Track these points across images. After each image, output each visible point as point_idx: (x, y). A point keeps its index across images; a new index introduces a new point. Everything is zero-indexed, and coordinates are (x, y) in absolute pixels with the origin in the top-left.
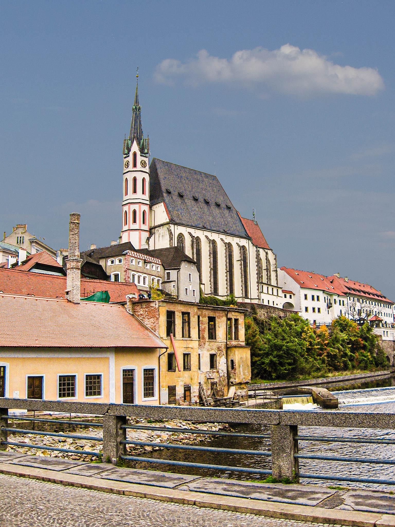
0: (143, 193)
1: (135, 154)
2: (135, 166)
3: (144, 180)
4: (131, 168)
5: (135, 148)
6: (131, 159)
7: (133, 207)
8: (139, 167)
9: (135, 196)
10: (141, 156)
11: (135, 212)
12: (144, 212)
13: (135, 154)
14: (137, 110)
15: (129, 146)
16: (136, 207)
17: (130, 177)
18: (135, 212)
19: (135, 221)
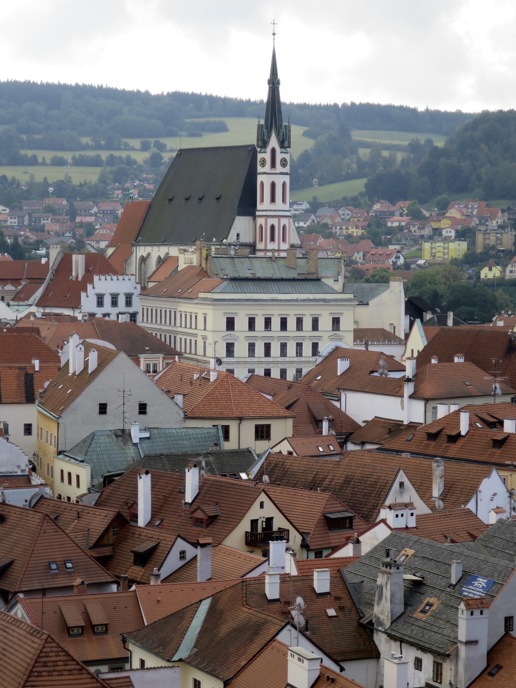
0: (283, 202)
1: (273, 151)
2: (273, 165)
3: (284, 184)
4: (267, 168)
5: (274, 142)
6: (267, 156)
7: (271, 221)
8: (279, 168)
9: (273, 207)
10: (282, 152)
11: (273, 227)
13: (273, 151)
14: (274, 83)
15: (265, 138)
16: (274, 221)
18: (273, 227)
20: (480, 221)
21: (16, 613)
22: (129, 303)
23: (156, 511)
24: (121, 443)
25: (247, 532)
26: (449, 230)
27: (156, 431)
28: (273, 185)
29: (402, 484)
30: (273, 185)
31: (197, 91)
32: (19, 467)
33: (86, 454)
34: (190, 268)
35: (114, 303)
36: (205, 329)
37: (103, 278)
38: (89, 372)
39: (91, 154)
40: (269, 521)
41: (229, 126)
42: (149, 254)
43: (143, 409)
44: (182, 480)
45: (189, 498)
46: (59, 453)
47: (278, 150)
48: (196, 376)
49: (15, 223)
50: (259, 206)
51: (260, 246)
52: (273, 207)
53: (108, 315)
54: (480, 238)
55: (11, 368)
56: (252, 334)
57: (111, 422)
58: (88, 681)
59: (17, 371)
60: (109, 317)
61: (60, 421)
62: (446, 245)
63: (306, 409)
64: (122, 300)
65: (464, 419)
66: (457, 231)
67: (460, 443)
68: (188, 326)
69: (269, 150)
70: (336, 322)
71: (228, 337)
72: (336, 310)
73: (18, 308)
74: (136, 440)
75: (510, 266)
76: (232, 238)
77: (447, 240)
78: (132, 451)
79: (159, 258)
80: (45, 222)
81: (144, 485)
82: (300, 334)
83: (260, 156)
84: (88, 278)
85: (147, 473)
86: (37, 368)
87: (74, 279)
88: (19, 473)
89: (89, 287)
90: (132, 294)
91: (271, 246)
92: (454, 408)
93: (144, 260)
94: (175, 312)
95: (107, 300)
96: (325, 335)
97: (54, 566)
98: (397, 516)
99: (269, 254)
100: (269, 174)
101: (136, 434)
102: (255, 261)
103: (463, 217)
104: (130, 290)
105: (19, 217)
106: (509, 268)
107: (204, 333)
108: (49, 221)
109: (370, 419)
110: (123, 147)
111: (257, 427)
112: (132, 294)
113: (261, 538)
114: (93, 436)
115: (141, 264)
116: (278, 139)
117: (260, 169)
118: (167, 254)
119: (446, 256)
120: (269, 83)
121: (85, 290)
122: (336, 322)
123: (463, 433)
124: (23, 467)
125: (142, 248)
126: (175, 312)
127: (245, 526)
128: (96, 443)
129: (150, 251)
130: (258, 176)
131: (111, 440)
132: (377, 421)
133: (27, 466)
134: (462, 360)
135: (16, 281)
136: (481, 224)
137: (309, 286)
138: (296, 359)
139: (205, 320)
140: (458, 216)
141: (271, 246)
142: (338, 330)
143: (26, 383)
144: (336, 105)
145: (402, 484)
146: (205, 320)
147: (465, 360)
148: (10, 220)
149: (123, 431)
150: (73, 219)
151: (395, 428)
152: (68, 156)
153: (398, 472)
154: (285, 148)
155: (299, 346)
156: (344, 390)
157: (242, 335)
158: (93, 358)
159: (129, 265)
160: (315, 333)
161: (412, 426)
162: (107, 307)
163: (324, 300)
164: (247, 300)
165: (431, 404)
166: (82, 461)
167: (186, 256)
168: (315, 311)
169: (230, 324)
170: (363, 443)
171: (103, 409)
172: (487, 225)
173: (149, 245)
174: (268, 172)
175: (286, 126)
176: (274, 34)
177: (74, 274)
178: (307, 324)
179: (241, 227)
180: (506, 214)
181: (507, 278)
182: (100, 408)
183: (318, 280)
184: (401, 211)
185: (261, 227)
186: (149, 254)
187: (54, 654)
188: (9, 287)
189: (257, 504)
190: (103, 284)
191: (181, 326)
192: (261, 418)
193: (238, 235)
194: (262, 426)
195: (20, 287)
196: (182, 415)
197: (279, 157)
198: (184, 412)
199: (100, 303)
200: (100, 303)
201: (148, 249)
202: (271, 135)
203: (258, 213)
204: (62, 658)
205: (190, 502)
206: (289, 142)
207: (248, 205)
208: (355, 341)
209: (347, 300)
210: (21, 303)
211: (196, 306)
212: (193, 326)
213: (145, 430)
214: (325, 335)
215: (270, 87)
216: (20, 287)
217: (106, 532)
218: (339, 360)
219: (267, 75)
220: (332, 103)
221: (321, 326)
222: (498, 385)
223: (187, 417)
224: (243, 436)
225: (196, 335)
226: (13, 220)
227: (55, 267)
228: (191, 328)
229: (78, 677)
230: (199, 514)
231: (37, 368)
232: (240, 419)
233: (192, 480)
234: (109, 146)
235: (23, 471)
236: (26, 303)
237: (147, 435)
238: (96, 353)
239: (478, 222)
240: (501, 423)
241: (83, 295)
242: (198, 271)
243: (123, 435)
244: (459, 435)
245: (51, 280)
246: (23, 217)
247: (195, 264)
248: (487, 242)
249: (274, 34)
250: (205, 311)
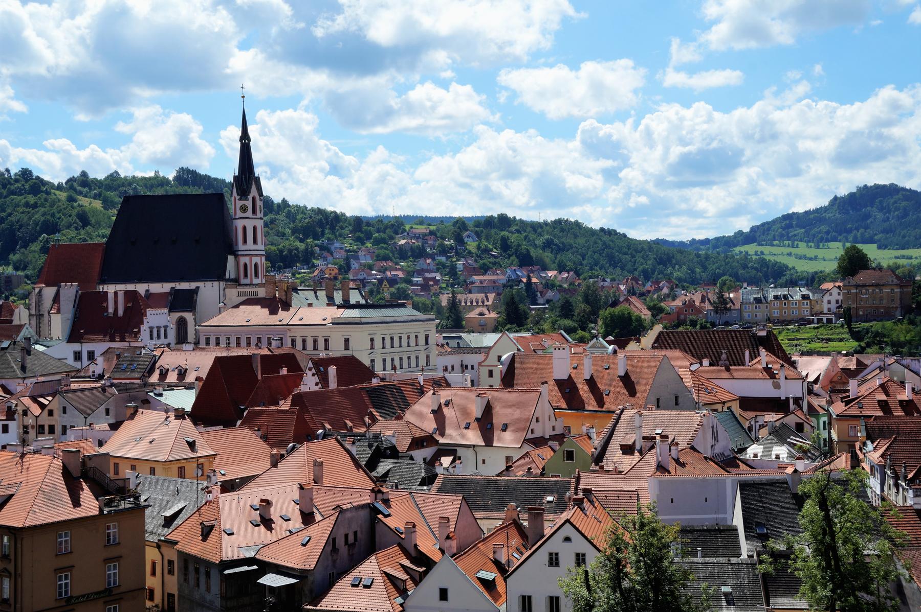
1: (254, 199)
4: (249, 213)
6: (249, 203)
8: (259, 215)
11: (256, 265)
13: (254, 199)
18: (256, 265)
19: (256, 275)
50: (241, 246)
69: (250, 197)
118: (147, 291)
177: (111, 310)
185: (245, 265)
202: (251, 186)
219: (240, 133)
249: (243, 97)
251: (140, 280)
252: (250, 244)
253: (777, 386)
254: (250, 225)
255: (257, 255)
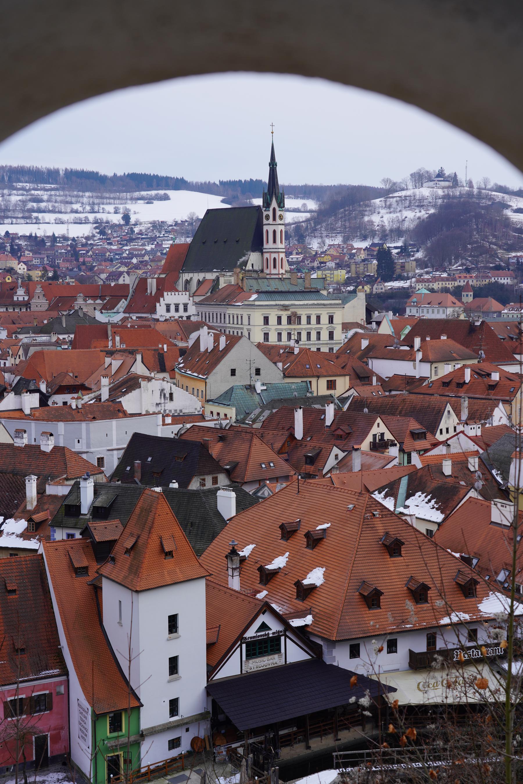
1: (274, 209)
2: (274, 219)
3: (281, 231)
4: (271, 221)
6: (271, 213)
7: (273, 255)
8: (278, 221)
9: (274, 246)
10: (280, 211)
11: (275, 259)
12: (282, 259)
13: (274, 209)
15: (269, 201)
17: (271, 229)
18: (275, 259)
19: (275, 267)
20: (350, 257)
21: (263, 493)
22: (186, 310)
23: (306, 432)
24: (250, 393)
25: (371, 442)
26: (330, 262)
27: (269, 385)
28: (274, 232)
29: (449, 412)
30: (274, 232)
31: (148, 173)
32: (196, 409)
33: (230, 401)
34: (230, 285)
35: (177, 310)
36: (249, 325)
37: (169, 293)
38: (220, 350)
39: (82, 216)
40: (382, 435)
41: (171, 197)
42: (191, 278)
43: (258, 372)
44: (324, 412)
45: (328, 422)
46: (208, 401)
47: (277, 209)
48: (282, 351)
49: (38, 262)
50: (265, 246)
51: (267, 271)
52: (274, 246)
53: (182, 317)
54: (353, 267)
55: (148, 350)
56: (279, 327)
57: (240, 381)
58: (397, 520)
59: (153, 352)
60: (182, 318)
61: (207, 381)
62: (332, 272)
63: (352, 370)
64: (181, 308)
65: (468, 372)
66: (336, 264)
67: (465, 387)
68: (235, 322)
69: (271, 209)
70: (331, 319)
71: (265, 329)
72: (331, 311)
73: (108, 314)
74: (259, 391)
75: (376, 285)
76: (249, 267)
77: (329, 269)
78: (257, 398)
79: (199, 280)
80: (59, 261)
81: (299, 415)
82: (309, 326)
83: (265, 214)
84: (160, 294)
85: (300, 408)
86: (165, 350)
87: (149, 295)
88: (197, 413)
89: (162, 299)
90: (188, 304)
91: (274, 271)
92: (459, 366)
93: (188, 282)
94: (225, 314)
95: (173, 308)
96: (324, 327)
97: (263, 466)
98: (471, 429)
99: (280, 276)
100: (272, 225)
101: (259, 388)
102: (271, 281)
103: (338, 254)
104: (186, 301)
105: (41, 258)
106: (375, 286)
107: (249, 327)
108: (61, 261)
109: (391, 375)
110: (101, 211)
111: (327, 381)
112: (188, 304)
113: (380, 445)
114: (232, 389)
115: (186, 285)
116: (277, 202)
117: (265, 222)
118: (204, 278)
119: (332, 279)
120: (270, 165)
121: (159, 302)
122: (331, 319)
123: (467, 381)
124: (198, 409)
125: (186, 274)
126: (225, 314)
127: (369, 438)
128: (235, 394)
129: (192, 276)
130: (264, 226)
131: (243, 392)
132: (396, 376)
133: (201, 408)
134: (445, 338)
135: (102, 298)
136: (351, 258)
137: (313, 295)
138: (316, 342)
139: (249, 318)
140: (335, 253)
141: (274, 271)
142: (332, 323)
143: (159, 359)
144: (240, 181)
145: (449, 412)
146: (249, 318)
147: (447, 338)
148: (34, 261)
149: (250, 385)
150: (77, 260)
151: (410, 382)
152: (64, 217)
153: (446, 405)
154: (281, 208)
155: (309, 334)
156: (371, 358)
157: (273, 328)
158: (223, 341)
159: (178, 285)
160: (318, 326)
161: (423, 379)
162: (173, 312)
163: (324, 305)
164: (276, 305)
165: (434, 365)
166: (229, 405)
167: (225, 279)
168: (318, 311)
169: (266, 320)
170: (390, 391)
171: (233, 372)
172: (355, 259)
173: (191, 272)
174: (271, 223)
175: (281, 194)
176: (272, 133)
177: (149, 291)
178: (313, 320)
179: (253, 259)
180: (366, 251)
181: (374, 293)
182: (231, 372)
183: (318, 292)
184: (297, 251)
185: (267, 259)
186: (191, 278)
187: (374, 505)
188: (99, 301)
189: (376, 425)
190: (169, 298)
191: (229, 323)
192: (330, 376)
193: (252, 264)
194: (331, 381)
195: (105, 301)
196: (282, 375)
197: (278, 213)
198: (284, 374)
199: (168, 310)
200: (168, 310)
201: (191, 275)
203: (264, 250)
204: (379, 508)
205: (329, 425)
206: (284, 204)
207: (258, 245)
208: (343, 330)
209: (337, 304)
210: (109, 311)
211: (242, 310)
212: (240, 322)
213: (263, 385)
214: (324, 327)
215: (270, 168)
216: (105, 301)
217: (283, 445)
218: (362, 340)
219: (269, 160)
220: (238, 180)
221: (321, 322)
222: (483, 352)
223: (285, 376)
224: (320, 387)
225: (242, 328)
226: (37, 261)
227: (134, 287)
228: (237, 324)
229: (391, 518)
230: (339, 432)
231: (165, 350)
232: (318, 377)
233: (330, 411)
234: (93, 211)
235: (198, 412)
236: (112, 311)
237: (265, 388)
238: (225, 337)
239: (349, 257)
240: (489, 375)
241: (158, 304)
242: (236, 288)
243: (251, 388)
244: (464, 383)
245: (132, 296)
246: (43, 258)
247: (233, 283)
248: (358, 269)
249: (272, 133)
250: (249, 313)
251: (201, 271)
252: (271, 244)
253: (415, 368)
254: (271, 229)
255: (275, 252)
